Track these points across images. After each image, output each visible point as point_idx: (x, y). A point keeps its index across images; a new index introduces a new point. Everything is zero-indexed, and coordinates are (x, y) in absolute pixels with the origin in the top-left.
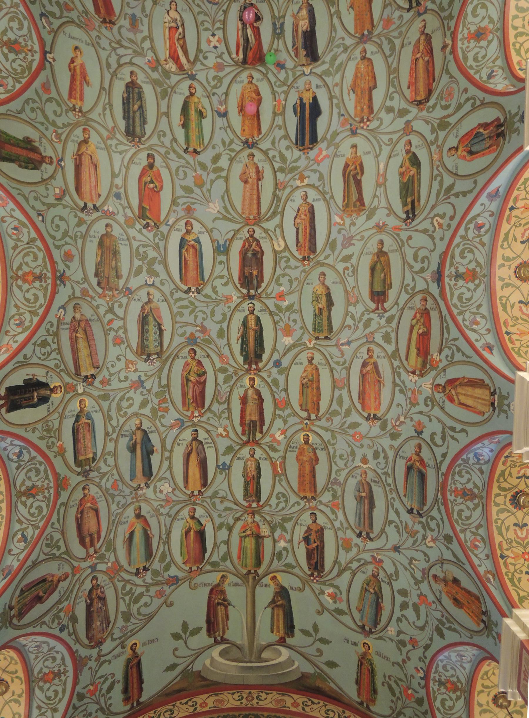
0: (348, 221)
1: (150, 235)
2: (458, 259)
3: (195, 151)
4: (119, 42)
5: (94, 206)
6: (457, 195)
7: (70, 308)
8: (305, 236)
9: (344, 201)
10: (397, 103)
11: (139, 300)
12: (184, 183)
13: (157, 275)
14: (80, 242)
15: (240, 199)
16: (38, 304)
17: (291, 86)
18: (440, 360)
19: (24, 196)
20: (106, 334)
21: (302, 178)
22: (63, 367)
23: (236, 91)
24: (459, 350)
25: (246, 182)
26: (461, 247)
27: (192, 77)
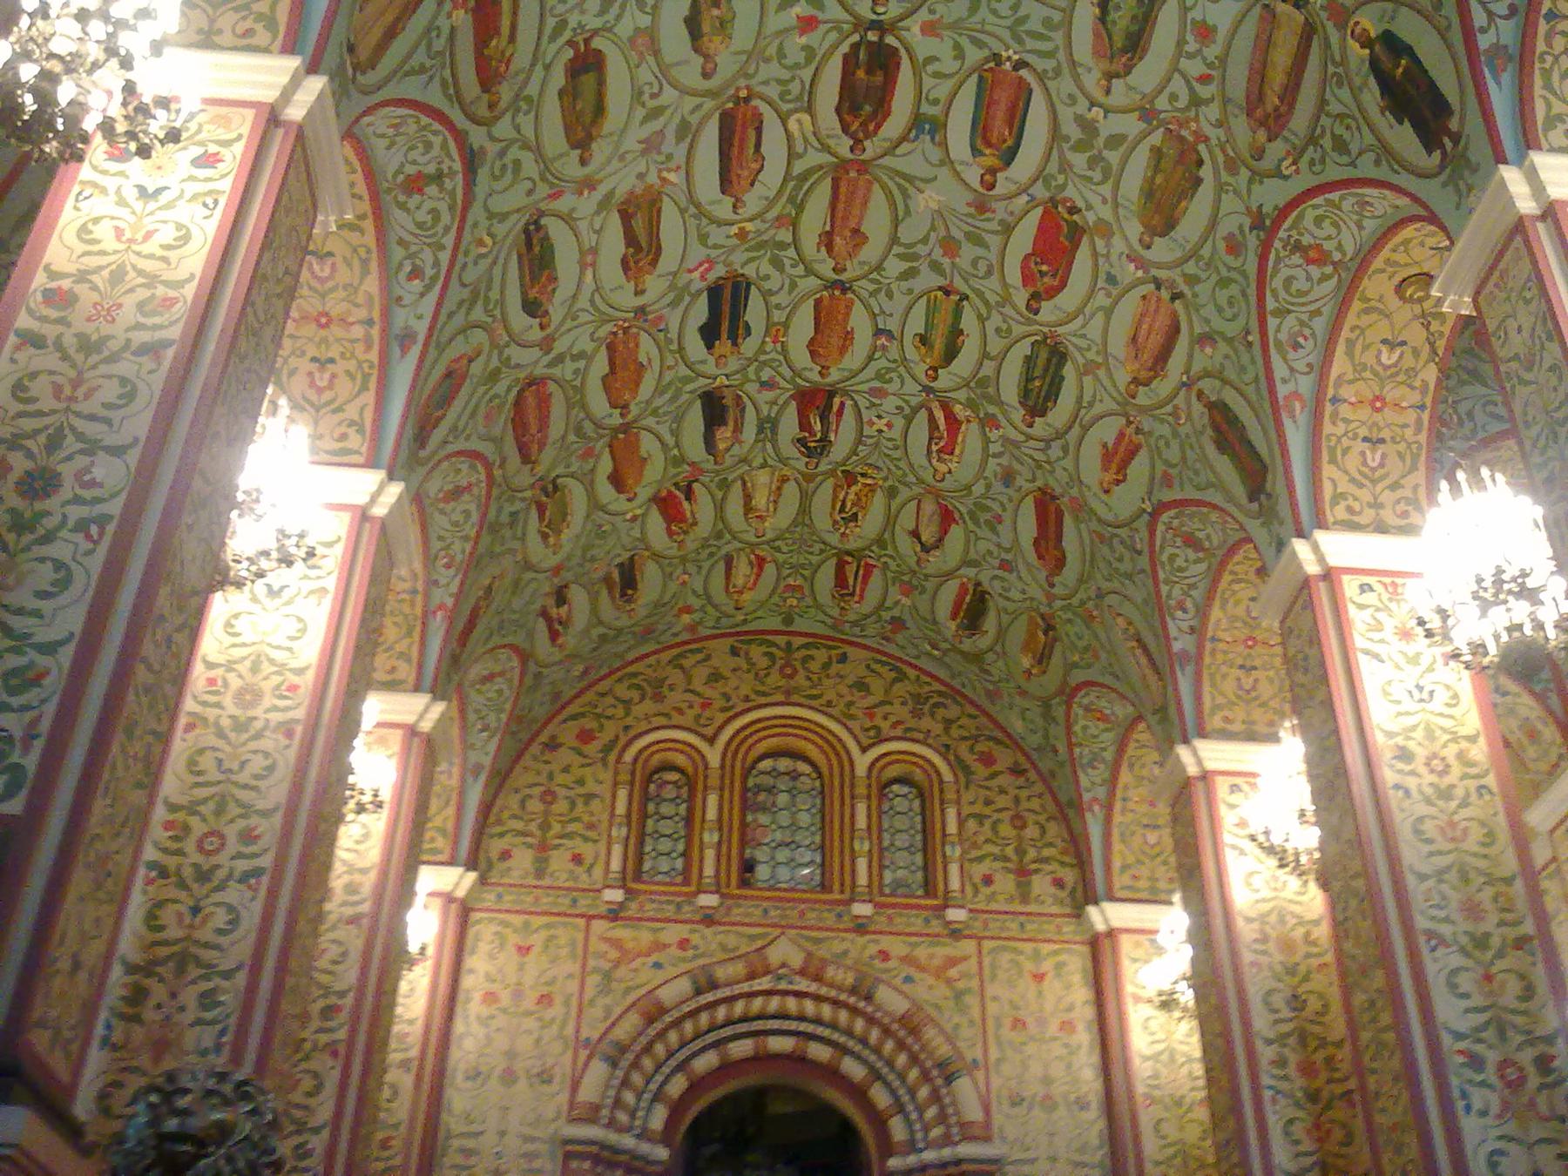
0: (652, 178)
1: (1070, 192)
2: (443, 207)
3: (947, 293)
4: (1040, 467)
5: (1158, 288)
6: (462, 302)
7: (1267, 164)
8: (743, 140)
9: (659, 211)
10: (567, 370)
11: (1131, 88)
12: (980, 252)
13: (1080, 121)
14: (1206, 252)
15: (871, 205)
16: (1320, 212)
17: (750, 361)
18: (449, 16)
19: (1258, 389)
20: (1223, 60)
21: (742, 235)
22: (1331, 69)
23: (853, 360)
24: (422, 70)
25: (856, 231)
26: (440, 229)
27: (928, 390)
